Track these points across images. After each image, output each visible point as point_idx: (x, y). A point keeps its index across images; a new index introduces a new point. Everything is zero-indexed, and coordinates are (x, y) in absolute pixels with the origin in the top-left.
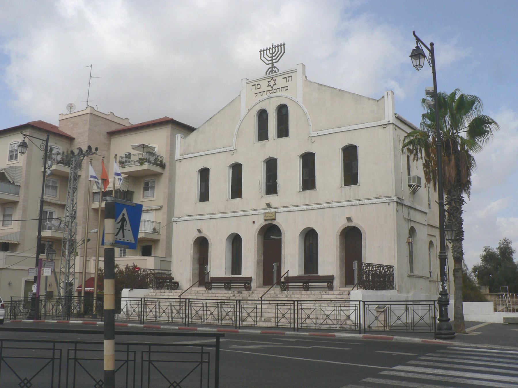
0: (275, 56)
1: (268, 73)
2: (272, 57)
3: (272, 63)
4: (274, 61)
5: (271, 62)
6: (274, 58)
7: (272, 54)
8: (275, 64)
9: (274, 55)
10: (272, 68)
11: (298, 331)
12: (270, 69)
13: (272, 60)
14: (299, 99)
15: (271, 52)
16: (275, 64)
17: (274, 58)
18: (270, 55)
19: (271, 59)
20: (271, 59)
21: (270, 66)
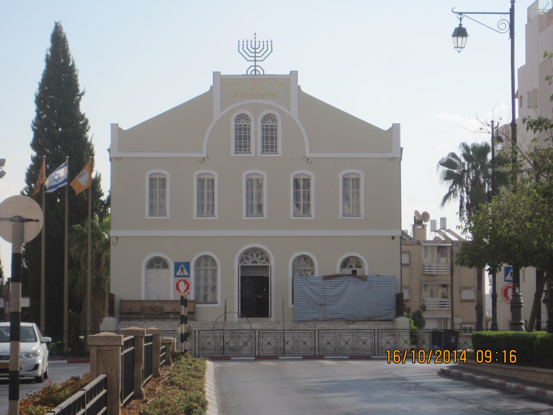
0: (259, 53)
1: (249, 73)
2: (255, 53)
3: (255, 61)
4: (257, 59)
5: (253, 59)
6: (257, 55)
7: (255, 49)
8: (258, 63)
9: (257, 51)
10: (255, 66)
11: (378, 355)
12: (253, 68)
13: (255, 57)
14: (294, 113)
15: (254, 47)
16: (258, 63)
17: (257, 55)
18: (253, 51)
19: (253, 55)
20: (253, 55)
21: (253, 63)
